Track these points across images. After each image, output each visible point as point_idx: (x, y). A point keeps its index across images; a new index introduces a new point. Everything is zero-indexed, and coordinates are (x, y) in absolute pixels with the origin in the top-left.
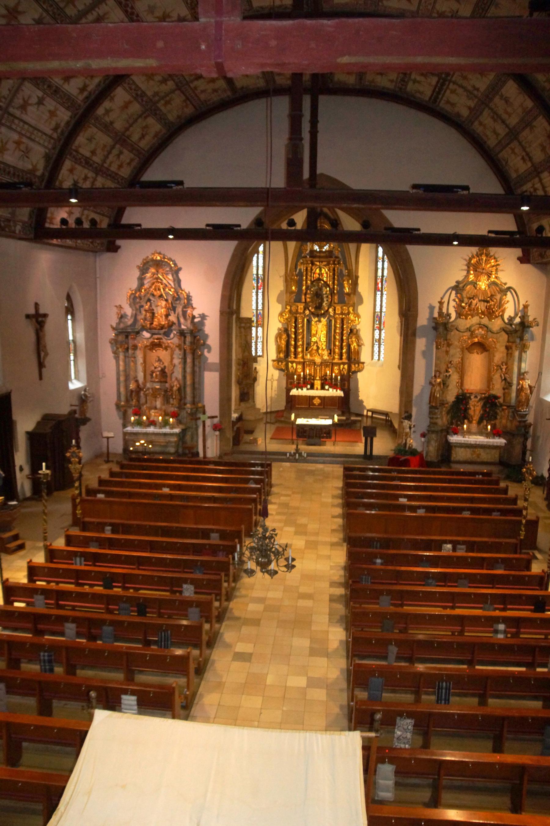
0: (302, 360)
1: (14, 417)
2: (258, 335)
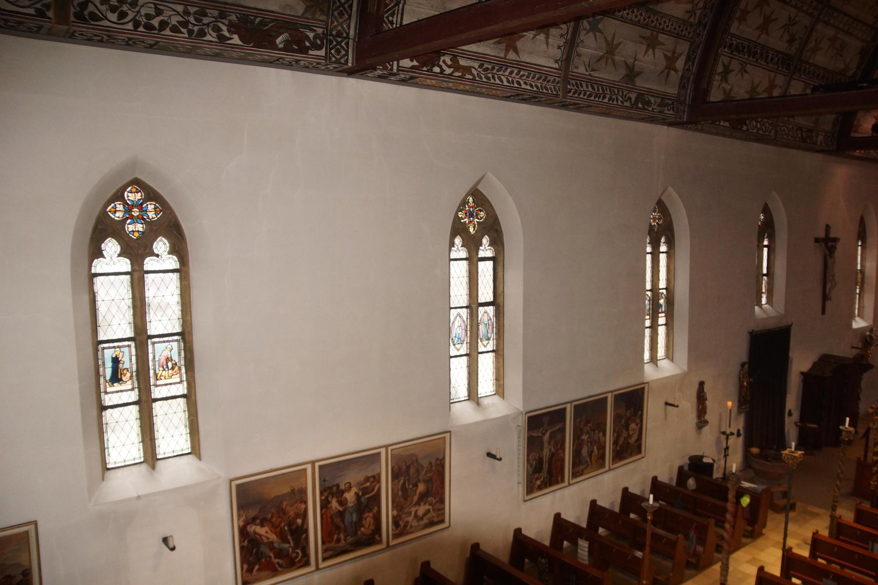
1: (791, 354)
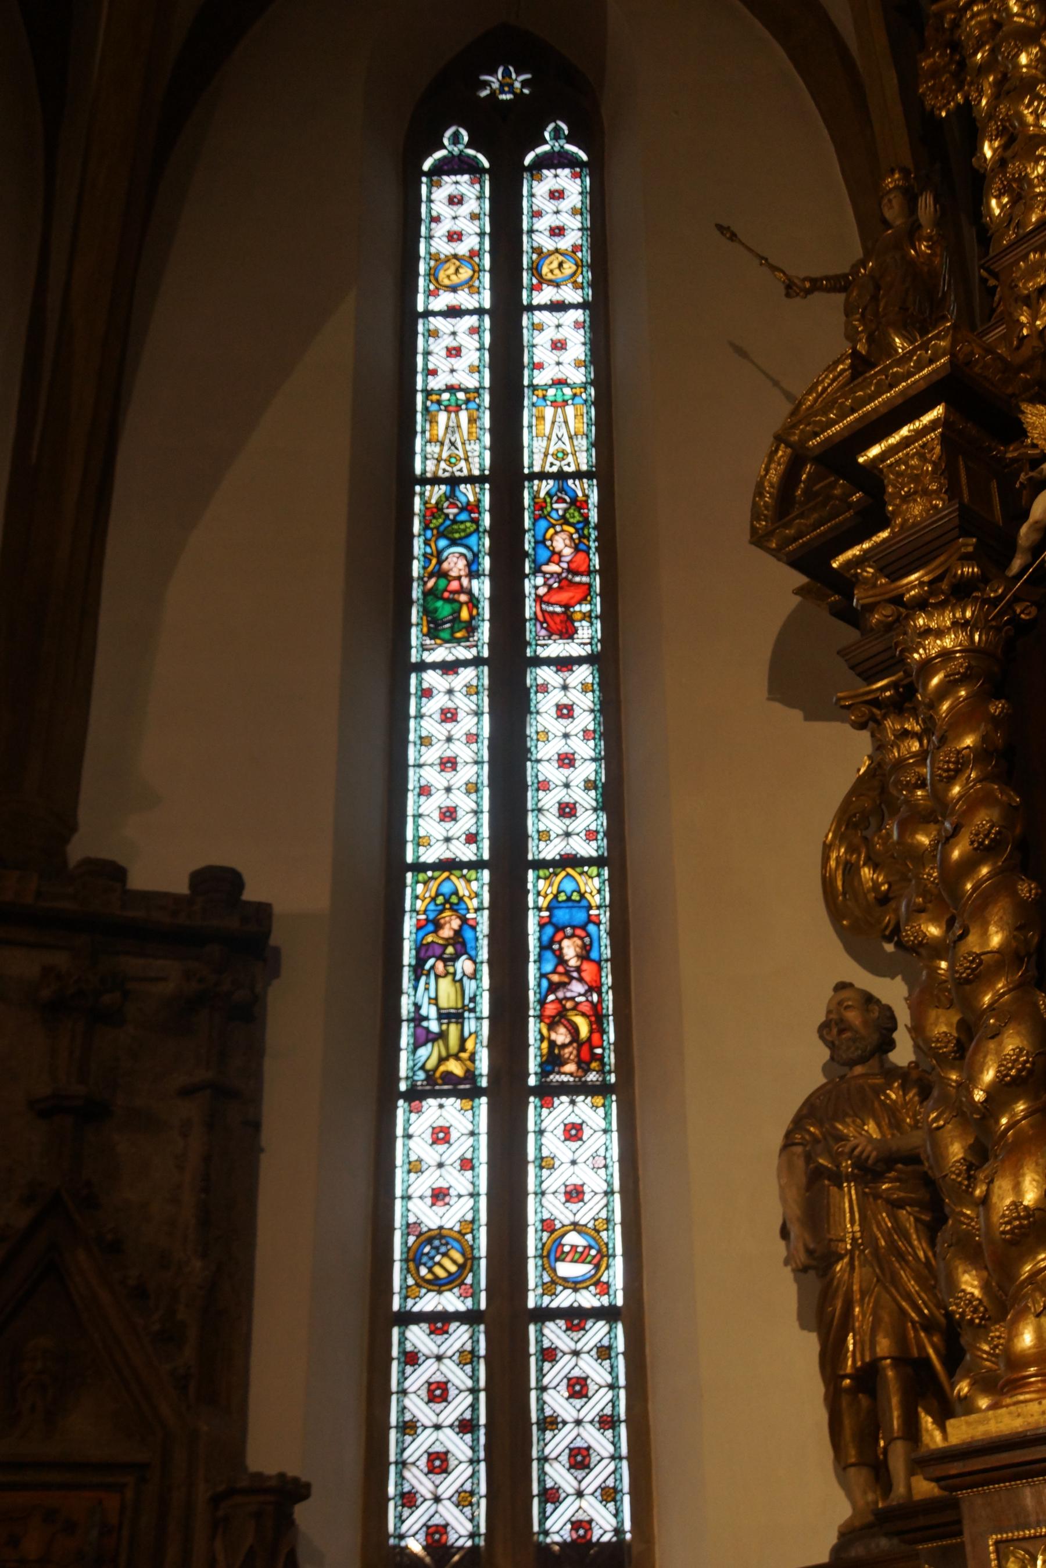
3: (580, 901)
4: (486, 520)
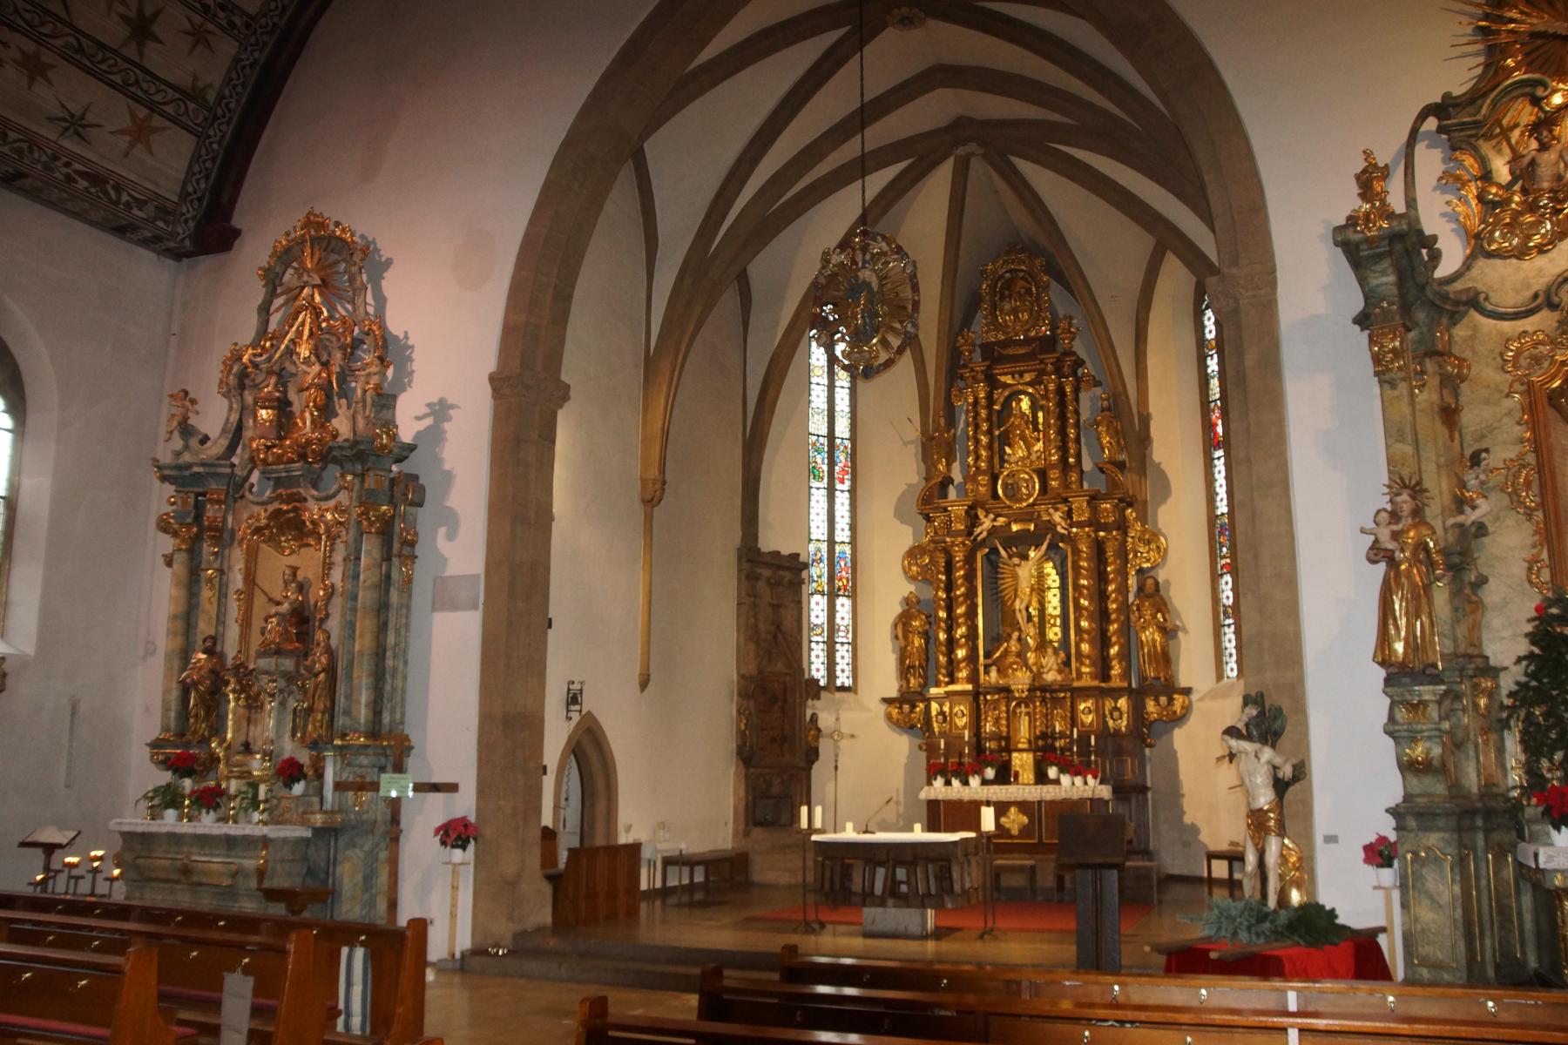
0: (969, 687)
2: (838, 620)
3: (844, 553)
4: (826, 449)
